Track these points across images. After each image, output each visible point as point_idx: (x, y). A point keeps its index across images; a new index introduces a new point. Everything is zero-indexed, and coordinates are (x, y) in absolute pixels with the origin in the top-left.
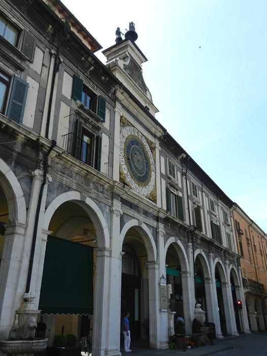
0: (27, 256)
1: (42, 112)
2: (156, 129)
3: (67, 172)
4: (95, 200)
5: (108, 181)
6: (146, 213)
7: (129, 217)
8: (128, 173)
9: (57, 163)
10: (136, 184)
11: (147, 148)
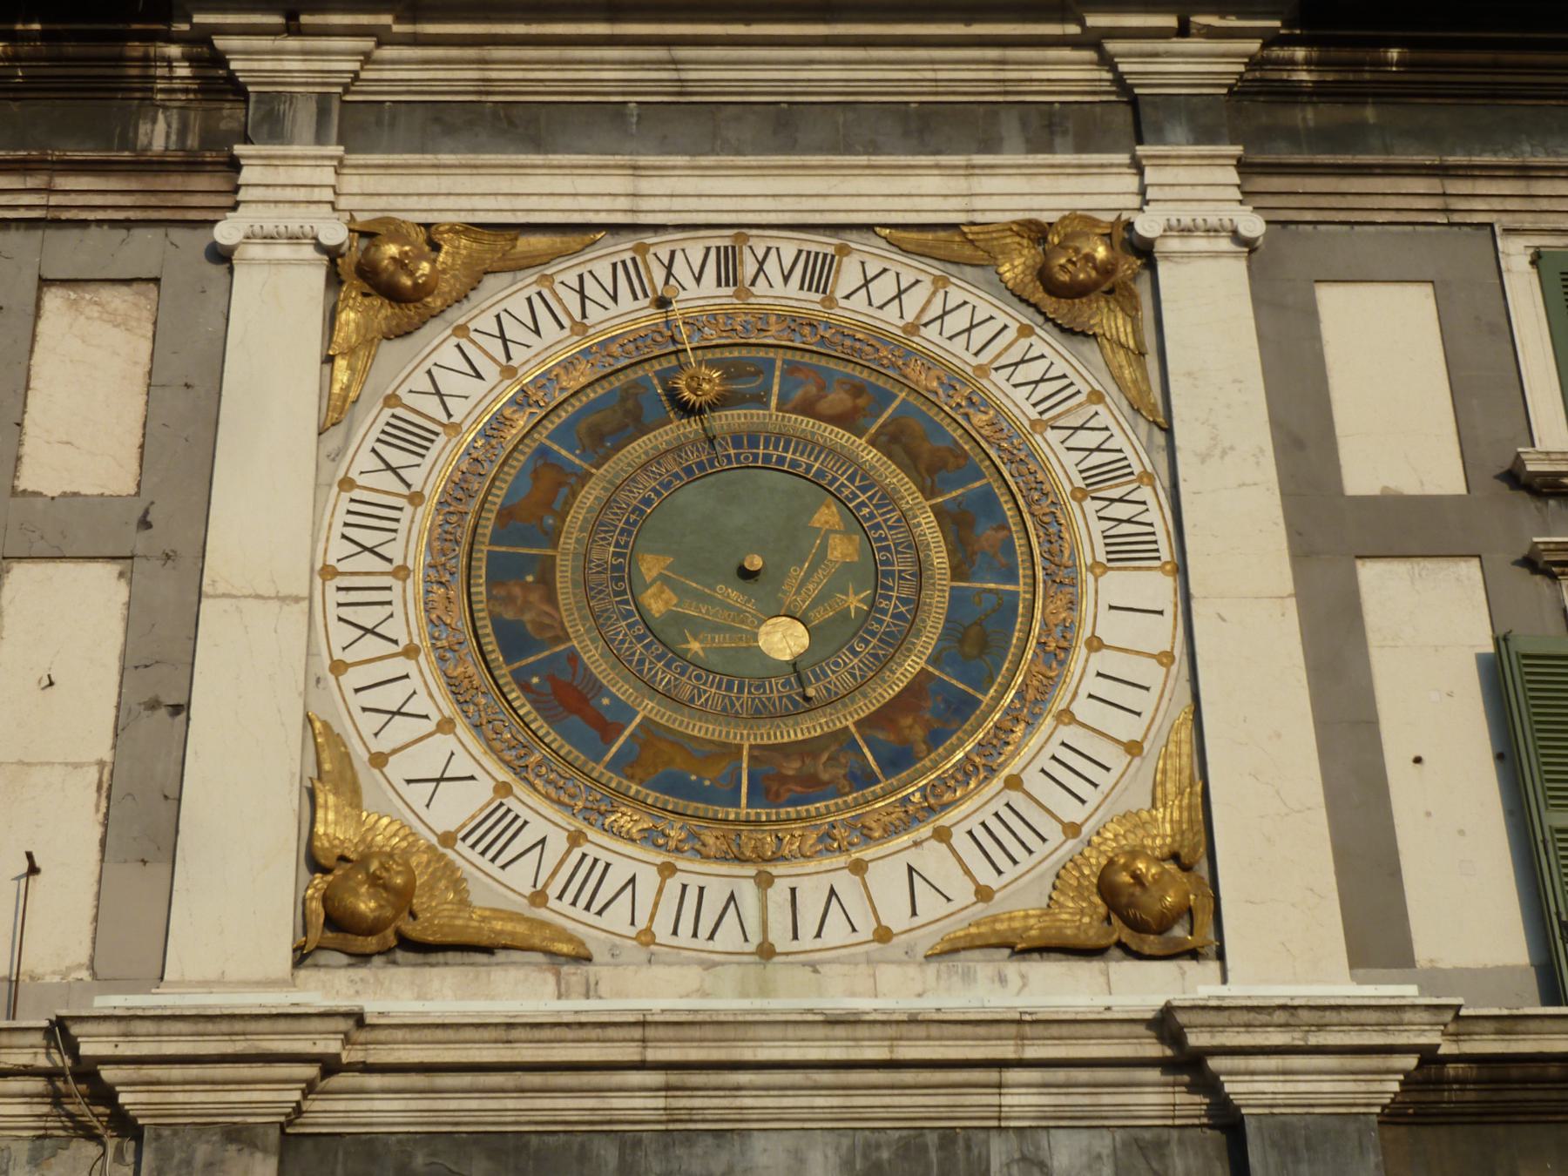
8: (526, 802)
10: (692, 871)
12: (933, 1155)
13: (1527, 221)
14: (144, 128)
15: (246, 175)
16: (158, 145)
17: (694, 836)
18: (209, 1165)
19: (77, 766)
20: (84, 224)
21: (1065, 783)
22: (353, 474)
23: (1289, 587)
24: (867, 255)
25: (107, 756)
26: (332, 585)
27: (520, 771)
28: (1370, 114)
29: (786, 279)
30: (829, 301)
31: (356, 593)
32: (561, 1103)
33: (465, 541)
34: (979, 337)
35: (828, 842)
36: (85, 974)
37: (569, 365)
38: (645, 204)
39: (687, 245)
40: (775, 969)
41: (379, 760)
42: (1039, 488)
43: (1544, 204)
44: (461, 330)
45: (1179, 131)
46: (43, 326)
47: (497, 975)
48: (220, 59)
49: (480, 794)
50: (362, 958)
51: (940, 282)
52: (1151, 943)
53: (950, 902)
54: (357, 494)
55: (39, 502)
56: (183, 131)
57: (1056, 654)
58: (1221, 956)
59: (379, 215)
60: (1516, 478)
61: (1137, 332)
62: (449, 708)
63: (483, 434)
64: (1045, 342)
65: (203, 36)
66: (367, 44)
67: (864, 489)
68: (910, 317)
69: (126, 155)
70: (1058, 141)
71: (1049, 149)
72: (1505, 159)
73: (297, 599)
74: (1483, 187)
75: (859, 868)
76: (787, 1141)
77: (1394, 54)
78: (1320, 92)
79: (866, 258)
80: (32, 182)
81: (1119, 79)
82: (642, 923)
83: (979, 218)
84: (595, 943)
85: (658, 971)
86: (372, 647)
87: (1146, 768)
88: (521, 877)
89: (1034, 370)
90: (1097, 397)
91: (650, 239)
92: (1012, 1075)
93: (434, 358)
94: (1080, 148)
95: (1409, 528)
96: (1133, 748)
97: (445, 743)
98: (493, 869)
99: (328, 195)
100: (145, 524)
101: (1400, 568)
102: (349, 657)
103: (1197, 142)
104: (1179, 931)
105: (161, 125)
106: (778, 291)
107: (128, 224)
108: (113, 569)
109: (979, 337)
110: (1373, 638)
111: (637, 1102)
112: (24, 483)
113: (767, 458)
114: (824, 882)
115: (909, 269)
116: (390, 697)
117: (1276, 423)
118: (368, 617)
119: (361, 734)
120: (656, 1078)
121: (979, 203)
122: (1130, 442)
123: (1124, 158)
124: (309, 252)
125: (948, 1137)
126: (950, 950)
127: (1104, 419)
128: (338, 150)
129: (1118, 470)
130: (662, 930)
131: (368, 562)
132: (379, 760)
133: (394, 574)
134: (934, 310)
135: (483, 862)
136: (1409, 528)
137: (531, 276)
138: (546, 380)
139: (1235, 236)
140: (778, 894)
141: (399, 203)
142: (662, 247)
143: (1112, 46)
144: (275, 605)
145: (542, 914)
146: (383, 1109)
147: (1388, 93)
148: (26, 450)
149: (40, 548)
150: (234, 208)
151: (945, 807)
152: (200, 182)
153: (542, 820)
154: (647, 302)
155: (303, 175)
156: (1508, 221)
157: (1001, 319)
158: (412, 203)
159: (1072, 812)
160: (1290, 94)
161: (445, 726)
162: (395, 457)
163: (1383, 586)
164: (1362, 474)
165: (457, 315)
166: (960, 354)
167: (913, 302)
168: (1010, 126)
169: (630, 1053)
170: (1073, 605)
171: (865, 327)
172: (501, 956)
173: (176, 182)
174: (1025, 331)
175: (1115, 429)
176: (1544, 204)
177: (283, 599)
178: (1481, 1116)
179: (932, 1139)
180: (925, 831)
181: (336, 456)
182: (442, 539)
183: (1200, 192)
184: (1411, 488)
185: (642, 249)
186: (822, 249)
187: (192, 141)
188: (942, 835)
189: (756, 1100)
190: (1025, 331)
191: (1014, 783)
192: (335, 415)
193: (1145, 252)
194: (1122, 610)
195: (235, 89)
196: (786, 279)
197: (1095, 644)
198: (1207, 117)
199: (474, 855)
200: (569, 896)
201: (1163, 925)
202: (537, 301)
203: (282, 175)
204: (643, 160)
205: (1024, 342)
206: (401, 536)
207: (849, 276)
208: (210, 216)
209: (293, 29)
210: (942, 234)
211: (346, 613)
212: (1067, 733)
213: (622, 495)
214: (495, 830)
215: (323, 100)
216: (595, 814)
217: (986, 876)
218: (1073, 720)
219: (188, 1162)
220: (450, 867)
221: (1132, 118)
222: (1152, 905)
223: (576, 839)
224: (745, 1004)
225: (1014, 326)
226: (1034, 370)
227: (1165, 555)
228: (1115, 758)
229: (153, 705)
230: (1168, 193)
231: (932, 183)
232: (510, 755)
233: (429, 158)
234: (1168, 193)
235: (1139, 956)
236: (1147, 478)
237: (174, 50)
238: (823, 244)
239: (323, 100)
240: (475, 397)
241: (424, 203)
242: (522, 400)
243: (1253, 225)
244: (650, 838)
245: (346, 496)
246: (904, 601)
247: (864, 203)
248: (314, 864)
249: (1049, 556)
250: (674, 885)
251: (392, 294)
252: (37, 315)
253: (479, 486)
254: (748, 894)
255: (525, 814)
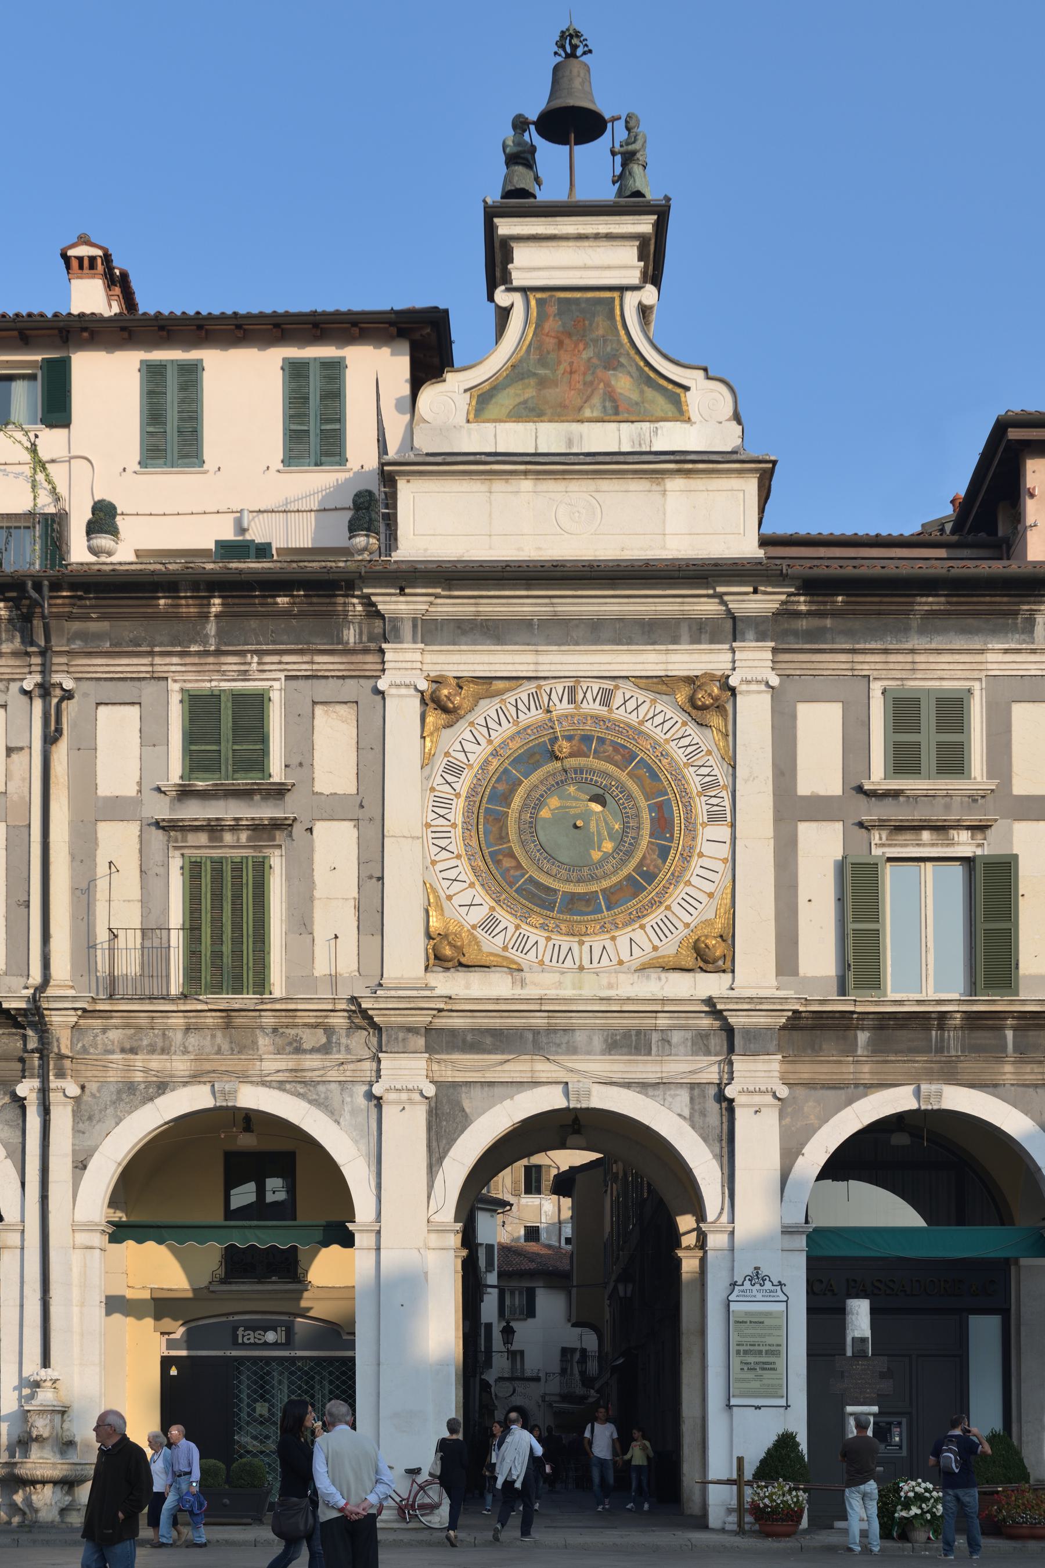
0: (34, 1290)
1: (27, 904)
2: (720, 596)
3: (145, 1042)
4: (288, 1086)
5: (330, 1007)
6: (631, 1040)
7: (498, 1090)
8: (501, 913)
9: (104, 1030)
11: (663, 723)
12: (634, 1038)
13: (883, 674)
14: (345, 632)
15: (388, 656)
16: (352, 640)
17: (557, 926)
18: (404, 1040)
19: (347, 899)
20: (327, 677)
21: (686, 908)
22: (435, 785)
23: (771, 834)
24: (626, 689)
25: (357, 896)
26: (429, 830)
27: (498, 902)
28: (828, 622)
29: (594, 700)
30: (610, 711)
31: (439, 834)
32: (514, 1021)
33: (476, 812)
34: (667, 726)
35: (603, 929)
36: (357, 974)
37: (512, 738)
38: (541, 668)
39: (557, 685)
40: (586, 976)
41: (449, 898)
42: (685, 791)
43: (891, 666)
44: (472, 724)
45: (750, 634)
46: (316, 722)
47: (492, 975)
48: (374, 605)
49: (484, 911)
50: (448, 969)
51: (653, 702)
52: (710, 967)
53: (643, 953)
54: (436, 794)
55: (323, 797)
56: (361, 634)
57: (686, 859)
58: (733, 971)
59: (438, 673)
60: (860, 789)
61: (726, 726)
62: (473, 879)
63: (481, 768)
64: (692, 729)
65: (368, 597)
66: (431, 599)
67: (621, 792)
68: (641, 718)
69: (340, 647)
70: (703, 636)
71: (699, 642)
72: (879, 646)
73: (418, 838)
74: (869, 658)
75: (613, 939)
76: (587, 1033)
77: (840, 599)
78: (809, 614)
79: (625, 691)
80: (306, 658)
81: (728, 610)
82: (540, 957)
83: (670, 673)
84: (525, 965)
85: (546, 975)
86: (444, 854)
87: (715, 903)
88: (499, 940)
89: (685, 742)
90: (709, 753)
91: (542, 682)
92: (659, 1015)
93: (462, 736)
94: (711, 643)
95: (819, 809)
96: (711, 895)
97: (471, 892)
98: (490, 938)
99: (419, 665)
100: (362, 806)
101: (814, 825)
102: (437, 858)
103: (757, 641)
104: (720, 963)
105: (352, 631)
106: (592, 707)
107: (343, 677)
108: (352, 824)
109: (667, 726)
110: (800, 853)
111: (539, 1021)
112: (317, 789)
113: (586, 779)
114: (602, 943)
115: (642, 696)
116: (452, 874)
117: (775, 765)
118: (443, 843)
119: (443, 888)
120: (546, 1014)
121: (670, 667)
122: (720, 773)
123: (727, 646)
124: (412, 691)
125: (638, 1032)
126: (642, 969)
127: (711, 762)
128: (422, 646)
129: (714, 784)
130: (547, 960)
131: (441, 821)
132: (449, 898)
133: (451, 826)
134: (650, 715)
135: (486, 935)
136: (819, 809)
137: (497, 700)
138: (504, 744)
139: (767, 684)
140: (586, 948)
141: (446, 667)
142: (546, 685)
143: (726, 598)
144: (410, 840)
145: (507, 954)
146: (458, 1022)
147: (835, 614)
148: (315, 775)
149: (325, 816)
150: (384, 670)
151: (644, 916)
152: (369, 658)
153: (506, 920)
154: (540, 711)
155: (409, 656)
156: (875, 674)
157: (676, 718)
158: (450, 667)
159: (687, 919)
160: (798, 614)
161: (472, 885)
162: (450, 778)
163: (806, 831)
164: (804, 787)
165: (470, 718)
166: (658, 734)
167: (643, 710)
168: (684, 630)
169: (537, 1007)
170: (694, 839)
171: (624, 722)
172: (493, 969)
173: (359, 658)
174: (685, 724)
175: (715, 766)
176: (891, 666)
177: (413, 838)
178: (813, 1028)
179: (633, 1033)
180: (637, 926)
181: (428, 778)
182: (468, 812)
183: (756, 664)
184: (822, 792)
185: (539, 687)
186: (609, 687)
187: (365, 638)
188: (642, 927)
189: (576, 1021)
190: (685, 724)
191: (668, 908)
192: (427, 760)
193: (733, 690)
194: (711, 839)
195: (379, 615)
196: (594, 700)
197: (701, 855)
198: (763, 628)
199: (483, 933)
200: (515, 948)
201: (715, 961)
202: (500, 711)
203: (401, 656)
204: (540, 648)
205: (684, 729)
206: (453, 811)
207: (618, 700)
208: (375, 674)
209: (402, 592)
210: (655, 680)
211: (436, 841)
212: (688, 889)
213: (533, 793)
214: (490, 924)
215: (414, 620)
216: (524, 918)
217: (657, 942)
218: (691, 884)
219: (397, 1039)
220: (475, 938)
221: (733, 629)
222: (709, 955)
223: (517, 927)
224: (574, 992)
225: (680, 721)
226: (685, 742)
227: (729, 819)
228: (703, 898)
229: (371, 877)
230: (744, 664)
231: (652, 657)
232: (494, 896)
233: (457, 648)
234: (744, 664)
235: (706, 972)
236: (725, 787)
237: (355, 601)
238: (608, 685)
239: (414, 620)
240: (478, 753)
241: (456, 667)
242: (495, 754)
243: (775, 681)
244: (543, 927)
245: (432, 794)
246: (633, 838)
247: (625, 667)
248: (429, 936)
249: (687, 819)
250: (550, 944)
251: (445, 710)
252: (313, 718)
253: (480, 790)
254: (576, 947)
255: (500, 918)
